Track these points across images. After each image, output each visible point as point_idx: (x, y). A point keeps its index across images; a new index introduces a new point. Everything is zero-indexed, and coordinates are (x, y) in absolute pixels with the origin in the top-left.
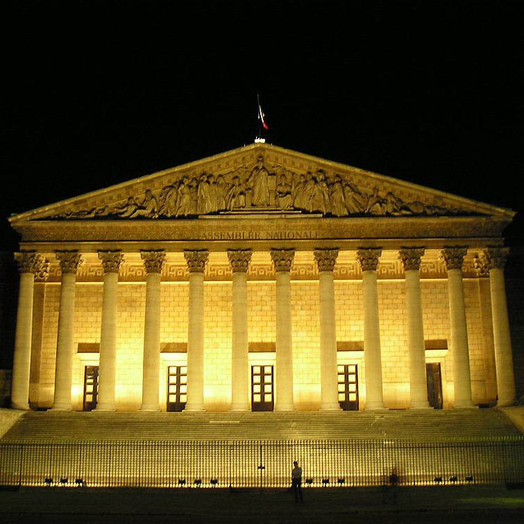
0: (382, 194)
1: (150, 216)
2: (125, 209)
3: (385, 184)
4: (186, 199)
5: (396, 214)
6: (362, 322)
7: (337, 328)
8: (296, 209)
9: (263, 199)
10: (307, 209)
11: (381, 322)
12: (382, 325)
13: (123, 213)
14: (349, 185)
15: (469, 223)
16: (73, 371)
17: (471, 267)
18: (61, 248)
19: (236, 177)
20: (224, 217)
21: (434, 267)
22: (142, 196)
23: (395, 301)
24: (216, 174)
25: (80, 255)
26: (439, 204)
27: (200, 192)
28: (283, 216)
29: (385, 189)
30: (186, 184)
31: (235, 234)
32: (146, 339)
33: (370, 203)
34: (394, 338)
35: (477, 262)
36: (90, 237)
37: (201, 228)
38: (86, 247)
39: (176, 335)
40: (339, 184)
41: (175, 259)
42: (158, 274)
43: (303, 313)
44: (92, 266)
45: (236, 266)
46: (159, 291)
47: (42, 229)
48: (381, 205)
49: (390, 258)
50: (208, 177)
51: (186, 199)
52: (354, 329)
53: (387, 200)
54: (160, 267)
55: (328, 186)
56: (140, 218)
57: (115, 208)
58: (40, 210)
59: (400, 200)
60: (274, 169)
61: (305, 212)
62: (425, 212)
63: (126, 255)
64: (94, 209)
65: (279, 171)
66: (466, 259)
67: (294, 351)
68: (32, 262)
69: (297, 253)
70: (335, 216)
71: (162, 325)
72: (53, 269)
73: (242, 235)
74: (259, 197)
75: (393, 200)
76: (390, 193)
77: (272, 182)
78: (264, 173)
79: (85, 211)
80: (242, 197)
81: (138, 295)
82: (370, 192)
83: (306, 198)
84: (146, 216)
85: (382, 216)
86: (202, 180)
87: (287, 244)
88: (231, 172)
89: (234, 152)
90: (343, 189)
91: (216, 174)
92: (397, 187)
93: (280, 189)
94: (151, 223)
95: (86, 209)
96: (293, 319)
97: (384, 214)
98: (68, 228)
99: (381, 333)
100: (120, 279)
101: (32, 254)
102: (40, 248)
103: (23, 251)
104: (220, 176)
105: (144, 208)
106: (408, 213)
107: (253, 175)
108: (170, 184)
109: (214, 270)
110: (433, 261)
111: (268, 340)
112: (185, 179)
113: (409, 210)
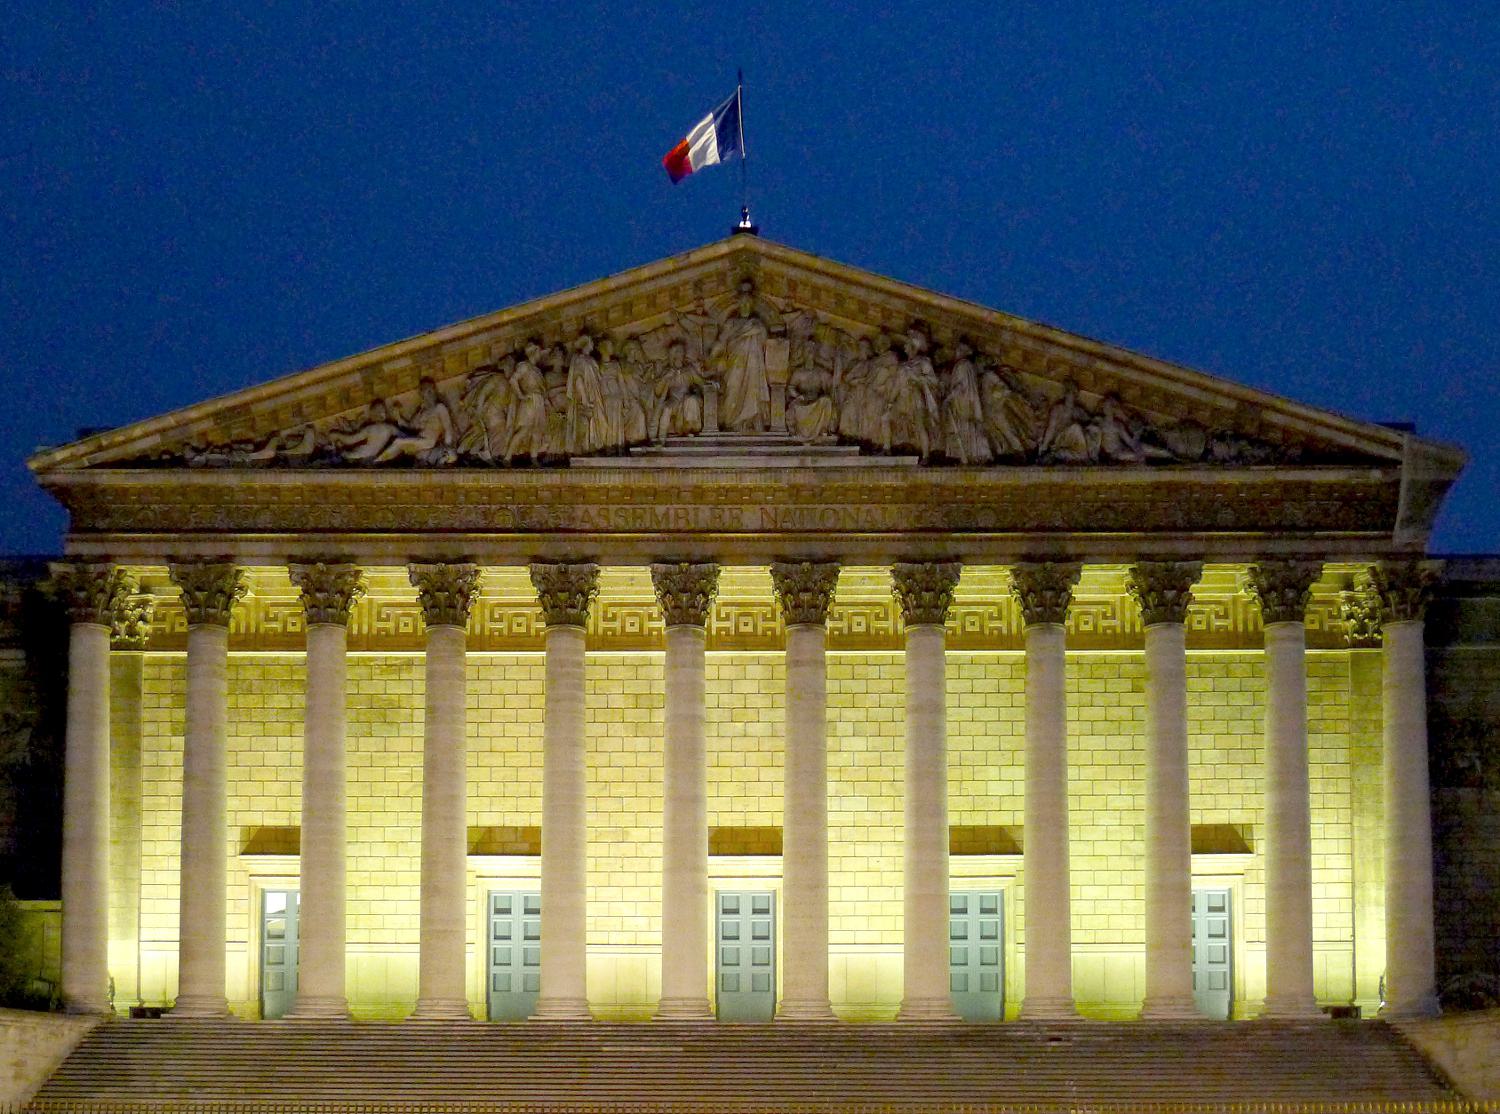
0: (1090, 398)
1: (432, 460)
2: (360, 437)
3: (1100, 365)
4: (533, 408)
5: (1129, 456)
6: (1020, 773)
7: (951, 789)
8: (843, 440)
9: (751, 410)
10: (874, 441)
11: (1072, 772)
12: (1077, 778)
13: (350, 448)
14: (996, 370)
15: (1331, 487)
16: (229, 906)
17: (1331, 616)
18: (183, 550)
19: (674, 343)
20: (643, 462)
21: (1226, 616)
23: (1114, 713)
24: (620, 331)
25: (239, 572)
26: (1250, 428)
27: (574, 385)
28: (809, 462)
29: (1099, 377)
30: (533, 360)
31: (672, 512)
32: (429, 817)
33: (1053, 423)
34: (1104, 819)
35: (1350, 600)
36: (264, 519)
37: (580, 494)
38: (255, 548)
39: (510, 804)
40: (968, 363)
41: (506, 587)
42: (457, 629)
43: (859, 743)
44: (274, 605)
45: (675, 607)
46: (461, 677)
47: (125, 491)
48: (1086, 432)
49: (1103, 587)
50: (596, 341)
51: (533, 408)
52: (991, 786)
53: (1103, 415)
54: (464, 608)
55: (938, 369)
56: (405, 462)
57: (333, 431)
59: (1137, 416)
60: (786, 318)
61: (868, 448)
62: (1208, 451)
63: (369, 573)
64: (274, 434)
65: (794, 321)
66: (1317, 591)
67: (832, 850)
68: (102, 590)
69: (845, 572)
70: (954, 462)
71: (472, 774)
72: (163, 611)
73: (692, 513)
74: (739, 409)
75: (1120, 414)
76: (1114, 396)
77: (778, 358)
78: (754, 331)
79: (248, 441)
80: (692, 403)
81: (404, 689)
82: (1054, 388)
83: (874, 406)
84: (423, 456)
85: (1086, 463)
86: (580, 351)
87: (820, 549)
88: (666, 326)
91: (620, 331)
92: (1134, 375)
93: (801, 377)
94: (437, 478)
95: (251, 435)
96: (831, 759)
97: (1094, 455)
98: (205, 491)
99: (1072, 803)
100: (353, 644)
101: (100, 567)
102: (124, 549)
103: (76, 559)
104: (633, 337)
105: (413, 433)
106: (1163, 453)
107: (723, 338)
108: (488, 362)
109: (614, 618)
110: (1226, 596)
111: (762, 821)
112: (531, 348)
113: (1163, 445)
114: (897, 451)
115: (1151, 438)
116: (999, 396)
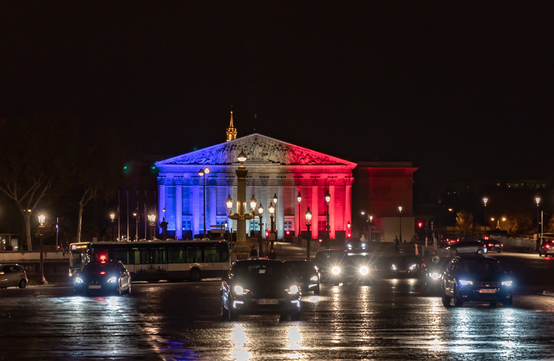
8: (270, 161)
9: (257, 157)
22: (208, 154)
58: (168, 160)
59: (311, 157)
61: (273, 162)
65: (263, 144)
82: (300, 153)
83: (274, 156)
89: (245, 137)
90: (289, 153)
91: (238, 145)
105: (209, 159)
114: (277, 163)
115: (314, 161)
116: (292, 155)
